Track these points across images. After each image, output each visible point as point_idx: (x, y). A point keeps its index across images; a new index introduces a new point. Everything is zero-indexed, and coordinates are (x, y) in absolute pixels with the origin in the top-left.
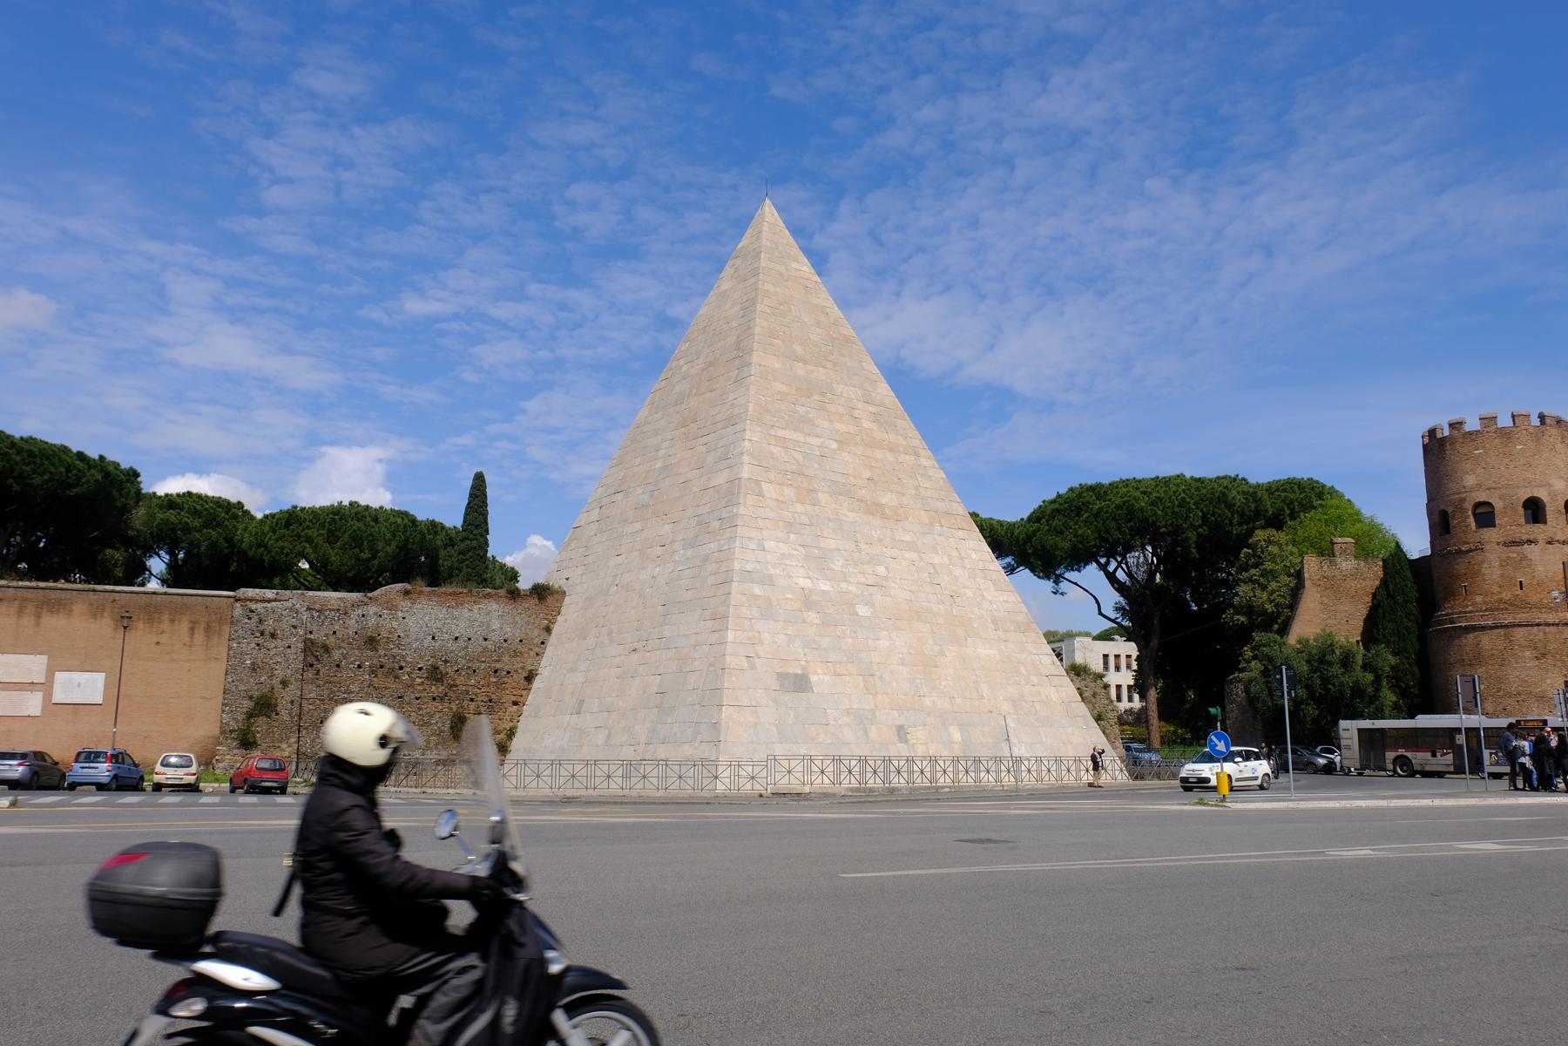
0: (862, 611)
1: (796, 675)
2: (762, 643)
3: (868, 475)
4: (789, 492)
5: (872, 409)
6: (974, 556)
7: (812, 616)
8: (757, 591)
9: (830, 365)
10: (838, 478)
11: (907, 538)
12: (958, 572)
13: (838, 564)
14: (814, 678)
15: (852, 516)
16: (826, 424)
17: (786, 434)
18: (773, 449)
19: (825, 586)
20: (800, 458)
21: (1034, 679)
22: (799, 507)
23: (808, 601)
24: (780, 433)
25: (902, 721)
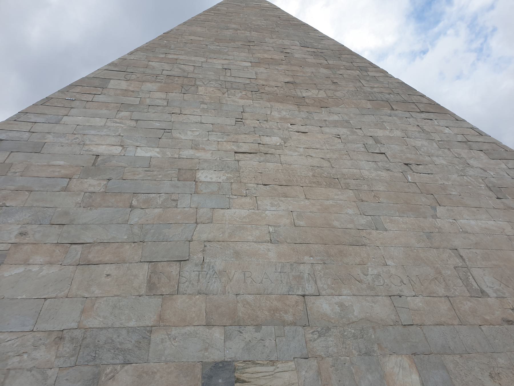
6: (447, 130)
7: (94, 184)
25: (233, 350)
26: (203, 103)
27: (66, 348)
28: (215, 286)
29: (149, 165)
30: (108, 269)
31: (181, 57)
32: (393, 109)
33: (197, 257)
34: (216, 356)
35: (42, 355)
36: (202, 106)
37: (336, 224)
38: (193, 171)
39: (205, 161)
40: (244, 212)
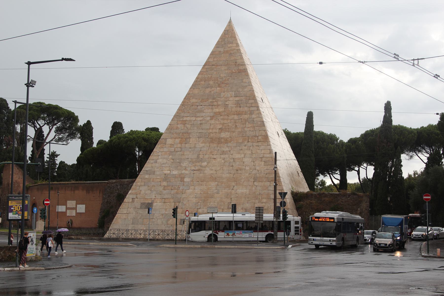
0: (186, 180)
1: (148, 203)
2: (140, 194)
3: (220, 127)
4: (178, 141)
5: (237, 99)
7: (165, 183)
8: (147, 176)
9: (223, 85)
10: (204, 131)
11: (227, 149)
12: (245, 160)
13: (185, 164)
14: (155, 204)
15: (202, 145)
16: (210, 110)
17: (188, 119)
18: (179, 126)
19: (175, 172)
20: (189, 126)
21: (264, 200)
22: (179, 145)
23: (166, 178)
24: (185, 119)
26: (190, 148)
27: (164, 216)
28: (184, 207)
29: (175, 176)
30: (168, 204)
31: (188, 119)
32: (248, 142)
33: (182, 201)
34: (182, 218)
35: (161, 217)
36: (190, 150)
37: (209, 193)
38: (184, 178)
39: (187, 174)
40: (192, 190)
